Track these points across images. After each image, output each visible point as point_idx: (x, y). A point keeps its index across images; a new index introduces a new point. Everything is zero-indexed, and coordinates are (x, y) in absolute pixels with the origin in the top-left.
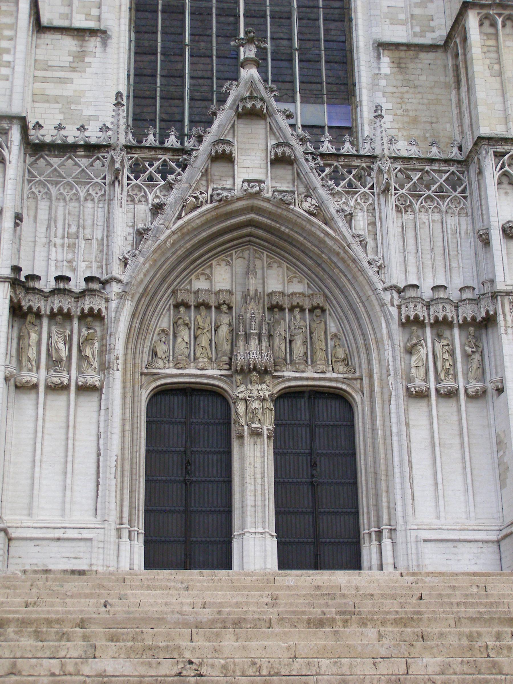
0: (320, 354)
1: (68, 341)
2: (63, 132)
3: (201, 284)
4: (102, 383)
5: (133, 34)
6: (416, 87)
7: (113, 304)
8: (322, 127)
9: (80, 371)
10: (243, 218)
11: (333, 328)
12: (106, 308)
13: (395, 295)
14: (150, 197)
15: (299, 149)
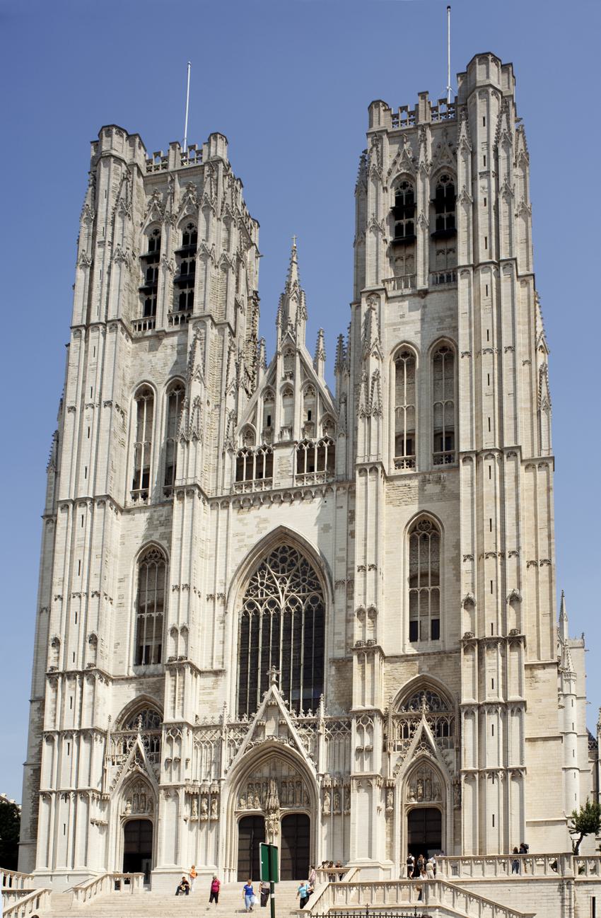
0: (298, 800)
1: (208, 804)
2: (206, 720)
3: (259, 775)
4: (219, 817)
5: (239, 666)
6: (345, 679)
7: (222, 789)
8: (311, 699)
9: (211, 815)
10: (269, 750)
11: (305, 788)
12: (220, 790)
13: (321, 778)
14: (236, 743)
15: (288, 720)
